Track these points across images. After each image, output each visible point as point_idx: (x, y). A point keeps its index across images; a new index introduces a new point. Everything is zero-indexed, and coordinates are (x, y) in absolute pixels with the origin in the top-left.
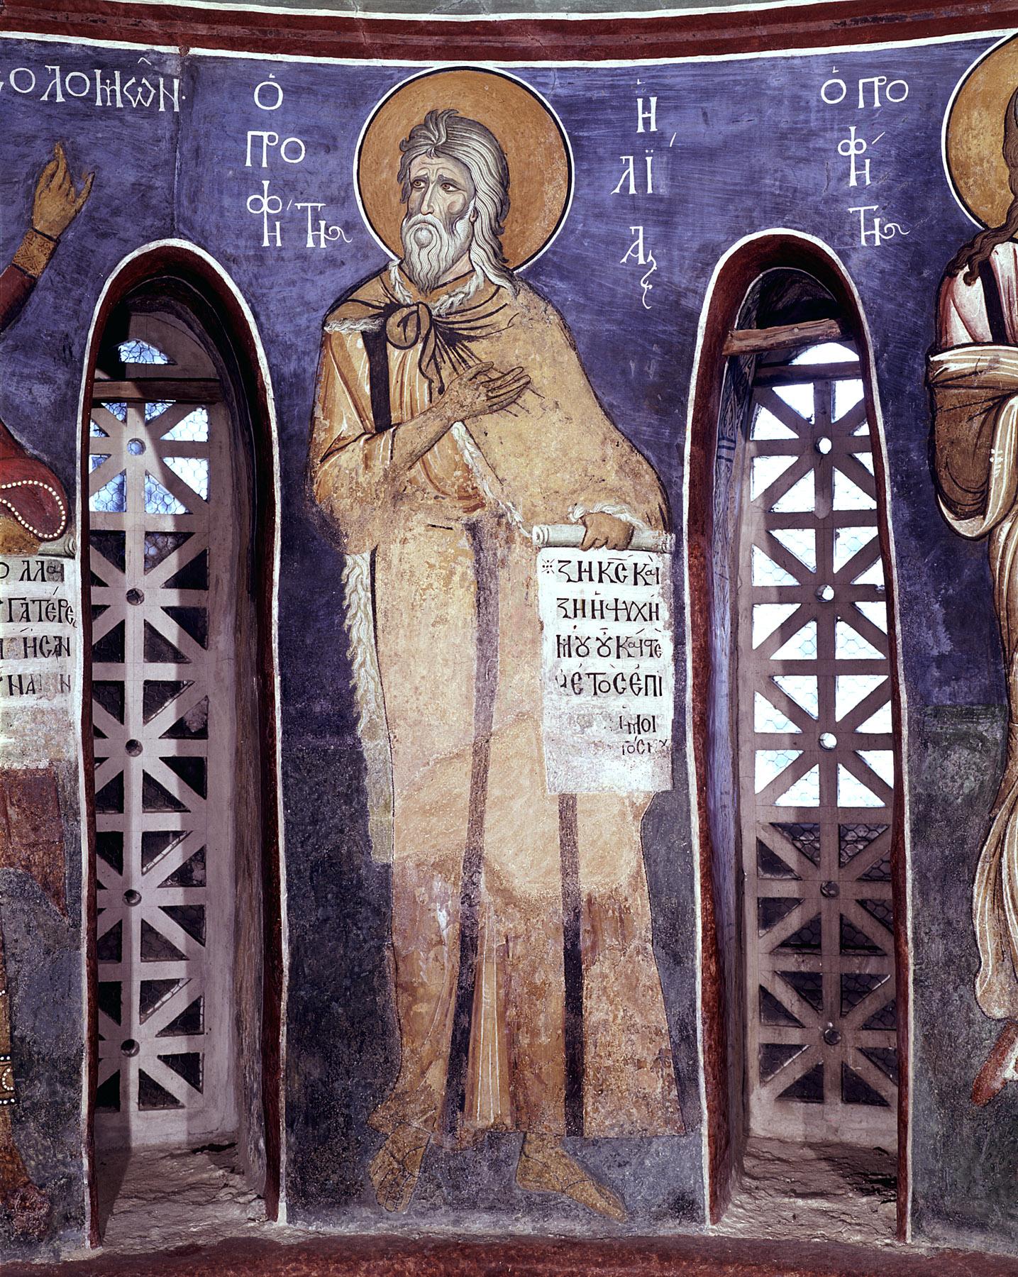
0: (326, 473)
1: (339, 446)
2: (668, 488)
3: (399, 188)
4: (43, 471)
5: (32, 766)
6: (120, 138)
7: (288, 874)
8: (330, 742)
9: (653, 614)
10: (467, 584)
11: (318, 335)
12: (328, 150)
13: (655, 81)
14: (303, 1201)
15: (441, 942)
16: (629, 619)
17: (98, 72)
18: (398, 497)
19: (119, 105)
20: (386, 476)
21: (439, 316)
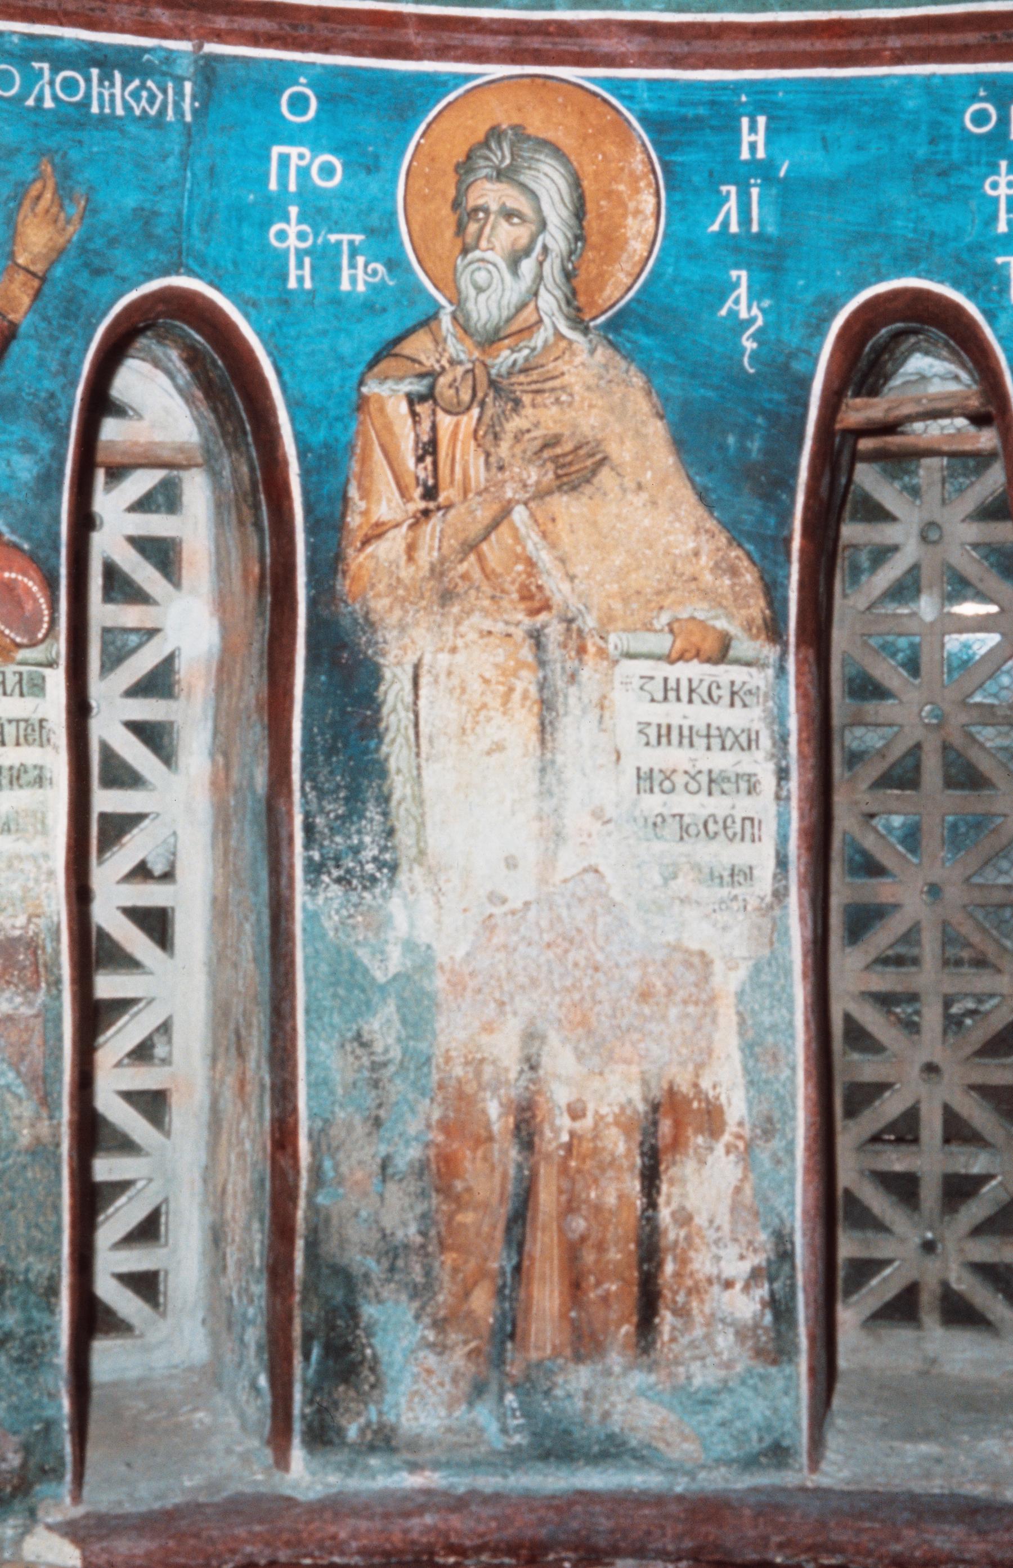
0: (360, 566)
1: (378, 532)
2: (772, 590)
3: (452, 219)
4: (20, 561)
6: (119, 151)
9: (752, 743)
10: (528, 703)
11: (354, 397)
13: (763, 97)
15: (490, 1139)
16: (723, 748)
17: (95, 72)
18: (447, 597)
20: (432, 570)
21: (499, 375)
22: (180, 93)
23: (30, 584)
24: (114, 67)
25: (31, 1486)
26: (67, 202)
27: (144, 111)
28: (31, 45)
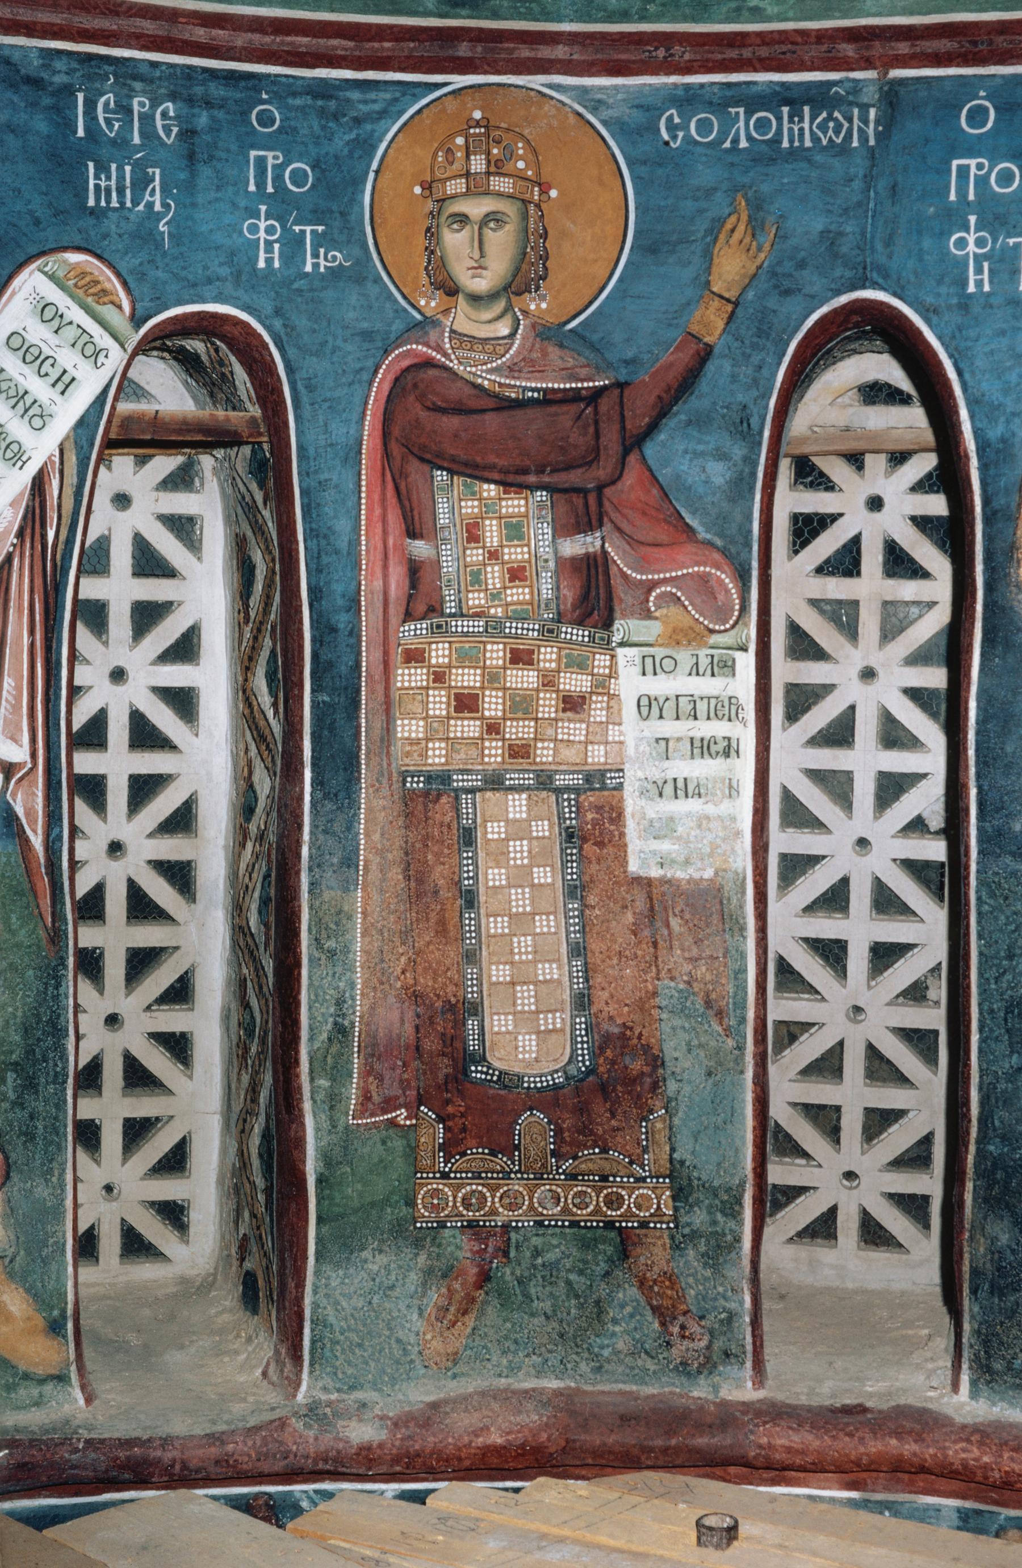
4: (717, 556)
5: (696, 875)
7: (981, 1013)
14: (987, 1375)
17: (785, 110)
19: (808, 143)
22: (865, 121)
23: (723, 576)
24: (804, 103)
25: (715, 1366)
27: (831, 140)
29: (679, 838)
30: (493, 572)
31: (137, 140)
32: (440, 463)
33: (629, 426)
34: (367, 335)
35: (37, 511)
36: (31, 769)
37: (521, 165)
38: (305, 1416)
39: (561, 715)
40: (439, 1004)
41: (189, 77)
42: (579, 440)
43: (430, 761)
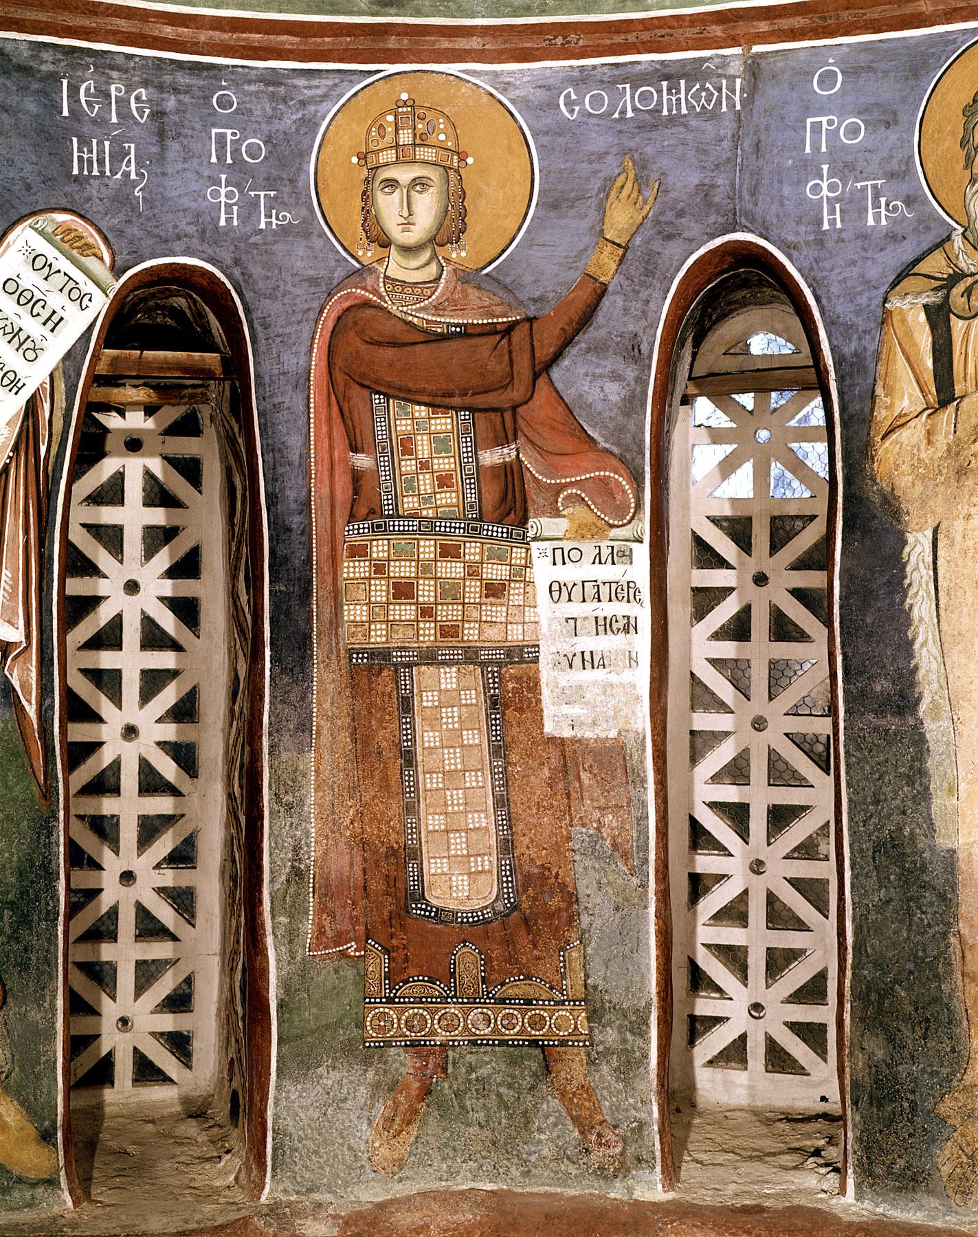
4: (615, 462)
5: (603, 735)
7: (852, 853)
8: (892, 723)
11: (879, 312)
12: (888, 125)
14: (870, 1178)
17: (665, 84)
19: (684, 111)
20: (949, 451)
24: (680, 78)
26: (643, 187)
27: (703, 107)
28: (617, 72)
29: (587, 704)
30: (424, 480)
31: (114, 120)
32: (378, 388)
33: (537, 355)
34: (313, 281)
35: (31, 429)
36: (26, 648)
37: (442, 137)
38: (268, 1215)
39: (484, 599)
40: (383, 850)
41: (159, 68)
42: (497, 367)
43: (372, 640)
